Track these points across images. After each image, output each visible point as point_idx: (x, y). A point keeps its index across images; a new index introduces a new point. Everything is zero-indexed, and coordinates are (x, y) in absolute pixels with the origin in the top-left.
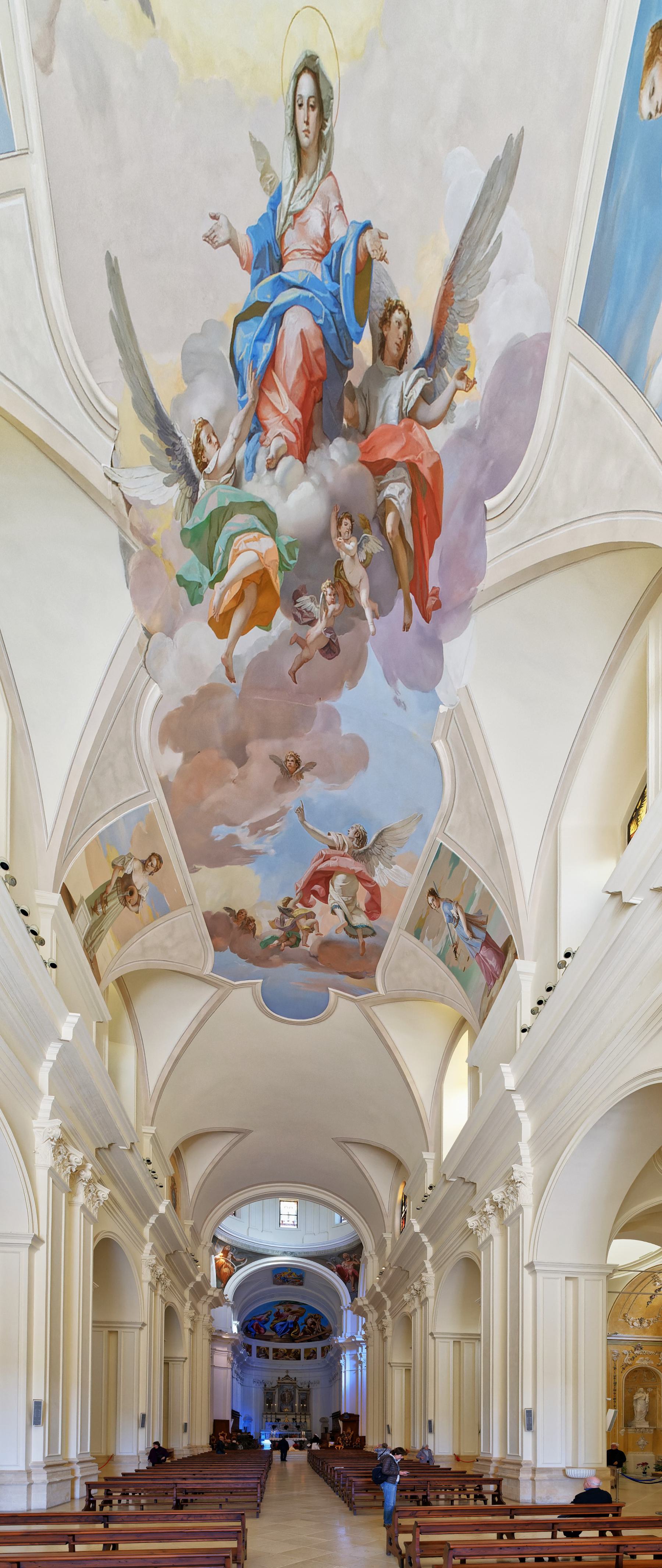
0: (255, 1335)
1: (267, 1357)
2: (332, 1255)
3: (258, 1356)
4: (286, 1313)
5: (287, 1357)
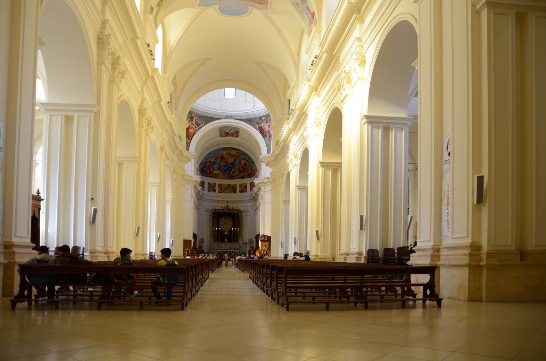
0: (207, 173)
1: (215, 191)
2: (256, 118)
3: (209, 191)
4: (227, 156)
5: (228, 191)
